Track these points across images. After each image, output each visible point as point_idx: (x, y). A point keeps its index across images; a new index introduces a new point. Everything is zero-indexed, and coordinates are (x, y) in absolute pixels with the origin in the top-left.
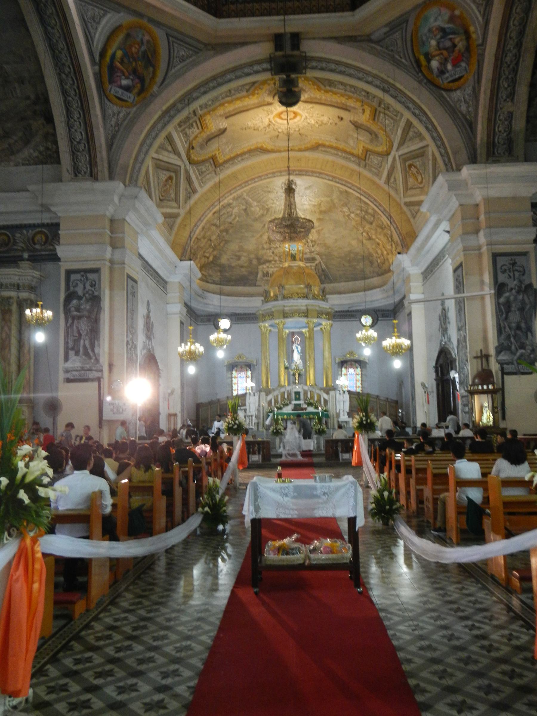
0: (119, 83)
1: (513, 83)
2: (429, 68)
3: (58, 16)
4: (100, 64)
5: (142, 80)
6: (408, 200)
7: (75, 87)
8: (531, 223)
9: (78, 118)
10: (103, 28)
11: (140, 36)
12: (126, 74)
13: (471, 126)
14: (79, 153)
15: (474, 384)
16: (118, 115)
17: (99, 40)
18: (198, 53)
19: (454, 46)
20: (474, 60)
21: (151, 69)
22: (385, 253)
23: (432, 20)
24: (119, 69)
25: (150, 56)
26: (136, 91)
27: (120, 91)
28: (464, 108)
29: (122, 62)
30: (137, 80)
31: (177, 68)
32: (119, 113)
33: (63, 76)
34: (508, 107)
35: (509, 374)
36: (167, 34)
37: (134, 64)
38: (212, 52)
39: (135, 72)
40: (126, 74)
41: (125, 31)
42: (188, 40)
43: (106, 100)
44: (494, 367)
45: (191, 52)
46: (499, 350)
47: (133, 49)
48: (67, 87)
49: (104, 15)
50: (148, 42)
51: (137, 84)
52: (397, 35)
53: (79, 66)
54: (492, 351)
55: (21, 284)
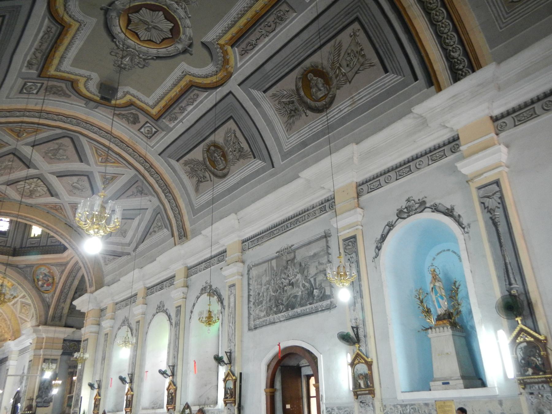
1: (66, 298)
2: (38, 283)
6: (21, 316)
8: (61, 348)
13: (49, 307)
15: (24, 411)
19: (48, 280)
20: (54, 287)
22: (3, 331)
23: (42, 270)
28: (48, 300)
34: (62, 305)
35: (39, 407)
44: (34, 404)
46: (37, 397)
52: (28, 269)
54: (35, 398)
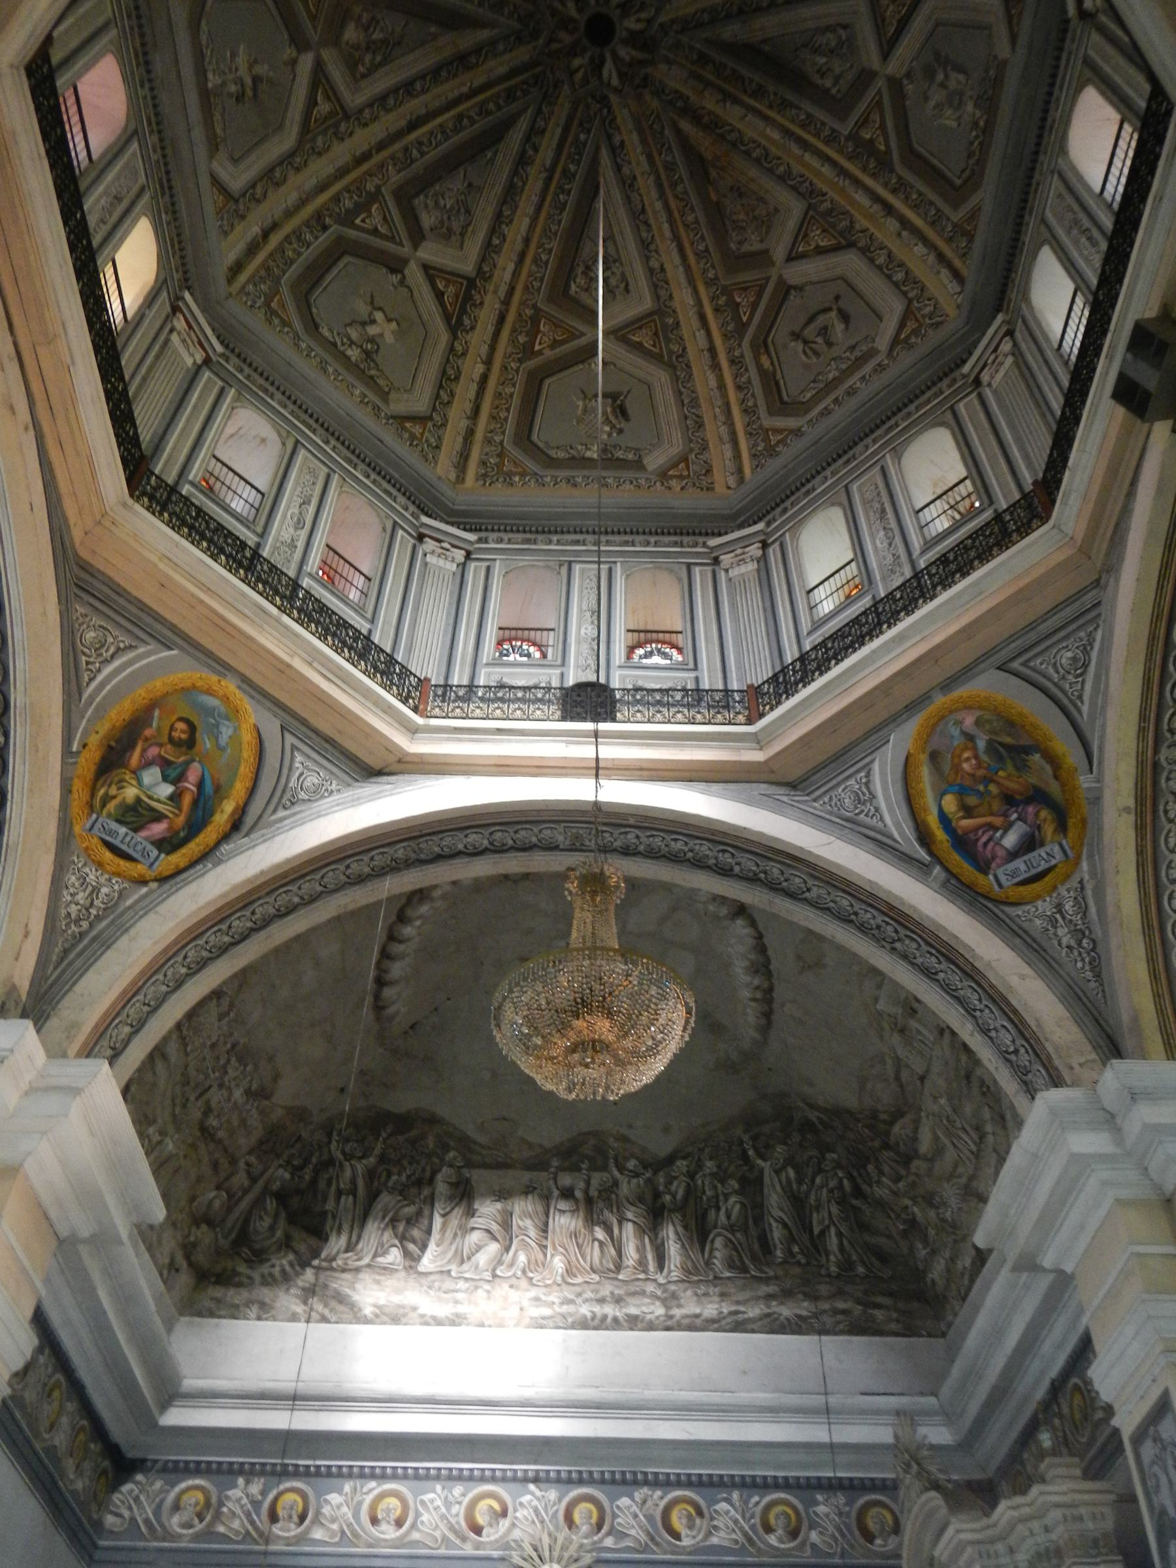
0: (1001, 853)
3: (789, 866)
4: (937, 859)
5: (1039, 796)
7: (925, 947)
9: (980, 1000)
10: (887, 798)
11: (956, 732)
12: (997, 821)
14: (1030, 1076)
16: (1060, 912)
17: (897, 825)
18: (1099, 615)
21: (1037, 757)
24: (976, 829)
25: (1008, 740)
26: (1049, 829)
27: (1019, 864)
29: (968, 811)
30: (1031, 809)
31: (1086, 697)
32: (1059, 908)
33: (898, 945)
36: (999, 668)
37: (993, 788)
38: (1112, 581)
39: (1009, 800)
40: (997, 821)
41: (924, 757)
42: (1044, 628)
43: (1007, 909)
45: (1082, 634)
47: (965, 766)
48: (919, 961)
49: (868, 775)
50: (978, 723)
51: (1037, 815)
53: (892, 907)
55: (1061, 1542)
